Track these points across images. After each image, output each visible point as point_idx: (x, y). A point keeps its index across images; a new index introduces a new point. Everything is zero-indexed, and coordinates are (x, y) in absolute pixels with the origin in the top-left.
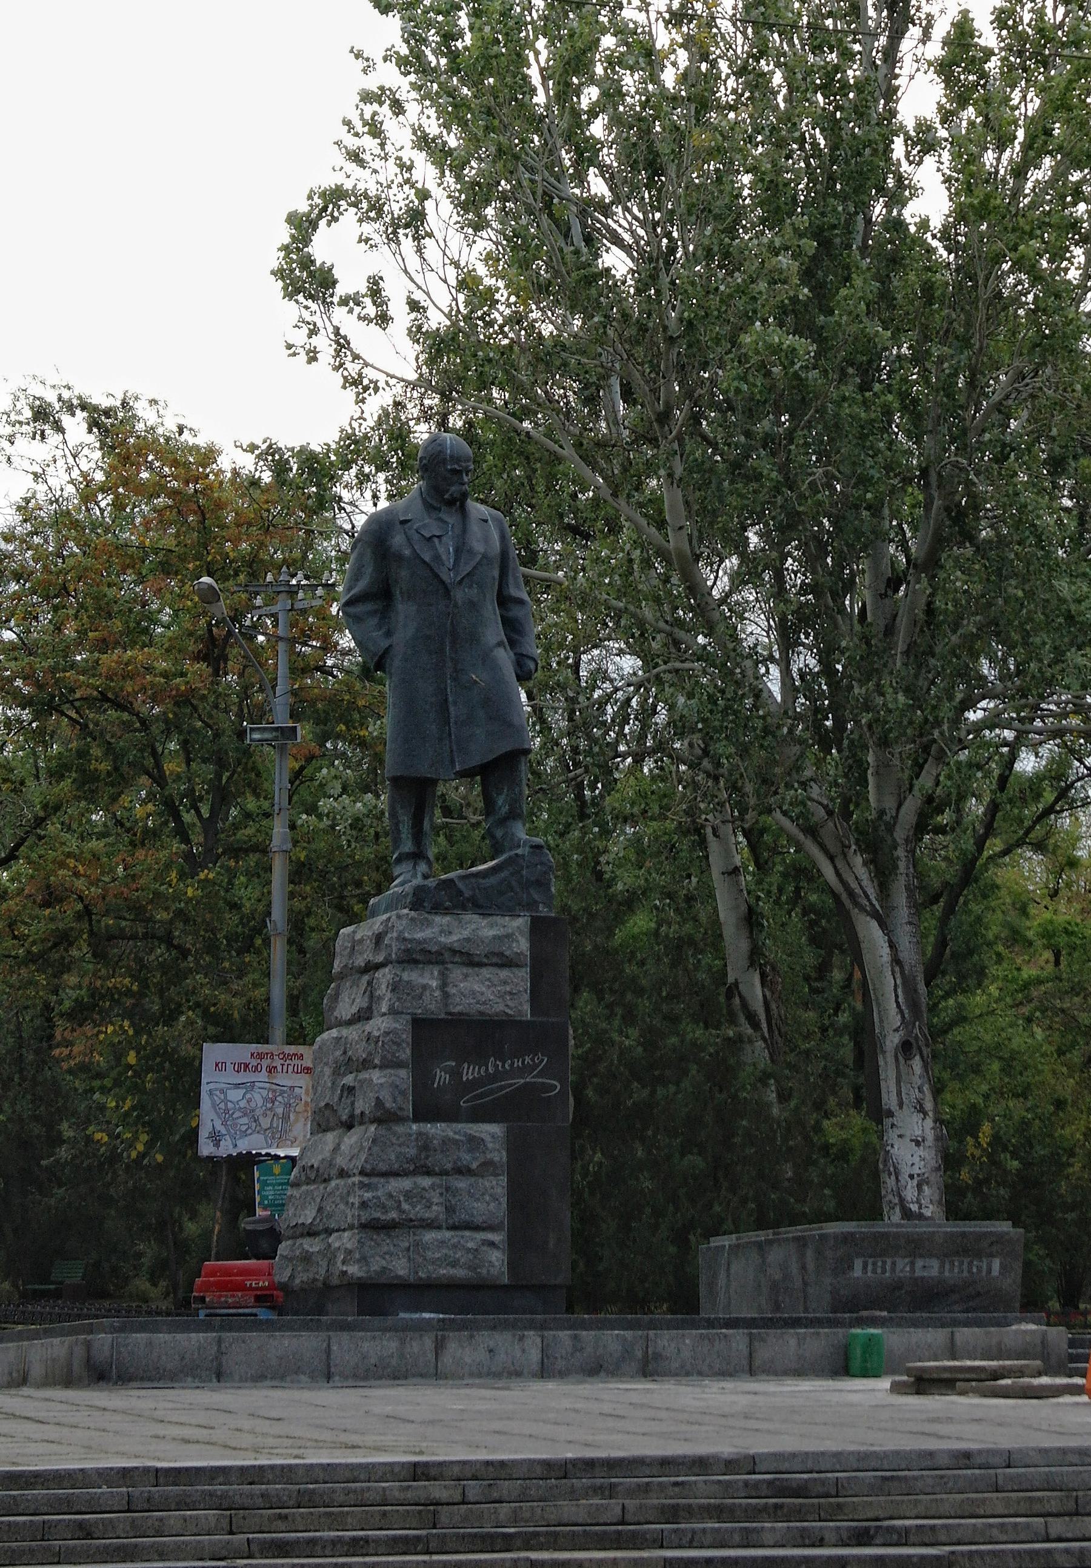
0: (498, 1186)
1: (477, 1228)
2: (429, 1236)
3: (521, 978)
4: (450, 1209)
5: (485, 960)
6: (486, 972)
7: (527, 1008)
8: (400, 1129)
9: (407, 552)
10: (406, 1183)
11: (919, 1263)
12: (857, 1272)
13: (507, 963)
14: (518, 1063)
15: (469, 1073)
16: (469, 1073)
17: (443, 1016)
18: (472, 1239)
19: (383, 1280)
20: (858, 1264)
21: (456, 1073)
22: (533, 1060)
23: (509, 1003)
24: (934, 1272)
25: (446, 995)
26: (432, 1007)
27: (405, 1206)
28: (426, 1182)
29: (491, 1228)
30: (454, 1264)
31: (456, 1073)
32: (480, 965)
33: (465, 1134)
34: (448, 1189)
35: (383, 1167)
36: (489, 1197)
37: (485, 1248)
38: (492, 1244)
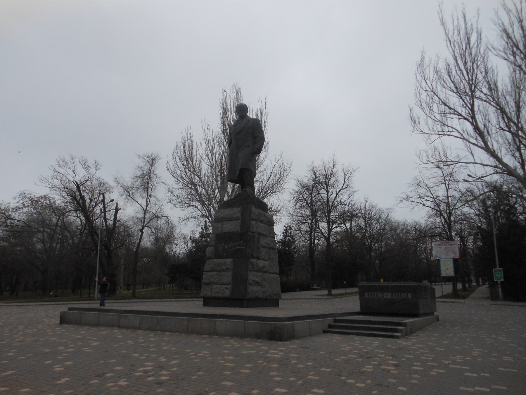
0: (229, 274)
1: (225, 284)
2: (216, 286)
3: (238, 223)
6: (231, 222)
7: (239, 230)
8: (211, 261)
10: (211, 274)
11: (385, 294)
12: (367, 296)
13: (236, 220)
14: (237, 244)
15: (227, 246)
20: (366, 294)
24: (390, 297)
28: (215, 273)
38: (227, 288)
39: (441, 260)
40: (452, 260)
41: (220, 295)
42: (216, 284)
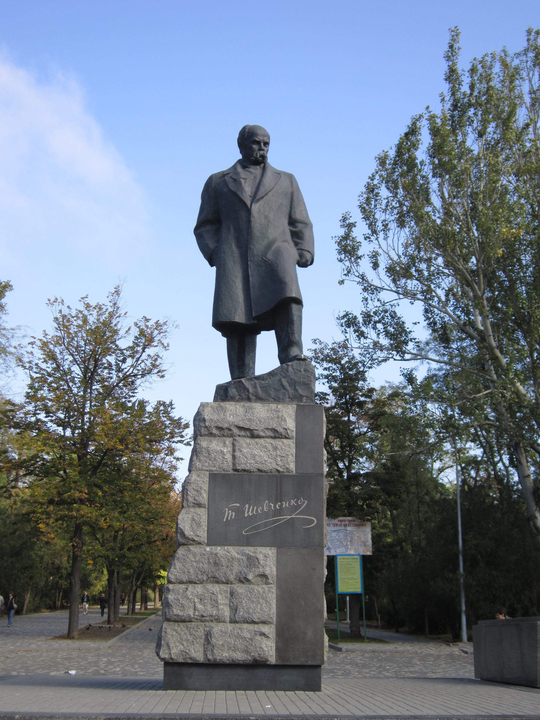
1: (253, 622)
2: (217, 628)
3: (289, 447)
4: (234, 609)
5: (262, 434)
6: (262, 441)
7: (292, 466)
9: (225, 190)
10: (199, 589)
15: (249, 511)
16: (249, 511)
17: (231, 472)
18: (247, 630)
19: (181, 660)
21: (239, 512)
22: (296, 502)
23: (280, 463)
25: (234, 457)
26: (225, 466)
27: (199, 606)
28: (216, 588)
29: (264, 623)
30: (235, 649)
31: (239, 512)
32: (259, 437)
33: (244, 554)
34: (232, 594)
35: (185, 578)
36: (265, 602)
37: (258, 638)
38: (263, 634)
39: (338, 557)
40: (358, 557)
41: (239, 656)
42: (218, 620)
